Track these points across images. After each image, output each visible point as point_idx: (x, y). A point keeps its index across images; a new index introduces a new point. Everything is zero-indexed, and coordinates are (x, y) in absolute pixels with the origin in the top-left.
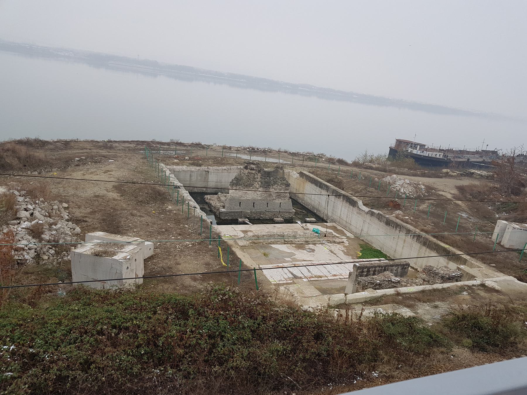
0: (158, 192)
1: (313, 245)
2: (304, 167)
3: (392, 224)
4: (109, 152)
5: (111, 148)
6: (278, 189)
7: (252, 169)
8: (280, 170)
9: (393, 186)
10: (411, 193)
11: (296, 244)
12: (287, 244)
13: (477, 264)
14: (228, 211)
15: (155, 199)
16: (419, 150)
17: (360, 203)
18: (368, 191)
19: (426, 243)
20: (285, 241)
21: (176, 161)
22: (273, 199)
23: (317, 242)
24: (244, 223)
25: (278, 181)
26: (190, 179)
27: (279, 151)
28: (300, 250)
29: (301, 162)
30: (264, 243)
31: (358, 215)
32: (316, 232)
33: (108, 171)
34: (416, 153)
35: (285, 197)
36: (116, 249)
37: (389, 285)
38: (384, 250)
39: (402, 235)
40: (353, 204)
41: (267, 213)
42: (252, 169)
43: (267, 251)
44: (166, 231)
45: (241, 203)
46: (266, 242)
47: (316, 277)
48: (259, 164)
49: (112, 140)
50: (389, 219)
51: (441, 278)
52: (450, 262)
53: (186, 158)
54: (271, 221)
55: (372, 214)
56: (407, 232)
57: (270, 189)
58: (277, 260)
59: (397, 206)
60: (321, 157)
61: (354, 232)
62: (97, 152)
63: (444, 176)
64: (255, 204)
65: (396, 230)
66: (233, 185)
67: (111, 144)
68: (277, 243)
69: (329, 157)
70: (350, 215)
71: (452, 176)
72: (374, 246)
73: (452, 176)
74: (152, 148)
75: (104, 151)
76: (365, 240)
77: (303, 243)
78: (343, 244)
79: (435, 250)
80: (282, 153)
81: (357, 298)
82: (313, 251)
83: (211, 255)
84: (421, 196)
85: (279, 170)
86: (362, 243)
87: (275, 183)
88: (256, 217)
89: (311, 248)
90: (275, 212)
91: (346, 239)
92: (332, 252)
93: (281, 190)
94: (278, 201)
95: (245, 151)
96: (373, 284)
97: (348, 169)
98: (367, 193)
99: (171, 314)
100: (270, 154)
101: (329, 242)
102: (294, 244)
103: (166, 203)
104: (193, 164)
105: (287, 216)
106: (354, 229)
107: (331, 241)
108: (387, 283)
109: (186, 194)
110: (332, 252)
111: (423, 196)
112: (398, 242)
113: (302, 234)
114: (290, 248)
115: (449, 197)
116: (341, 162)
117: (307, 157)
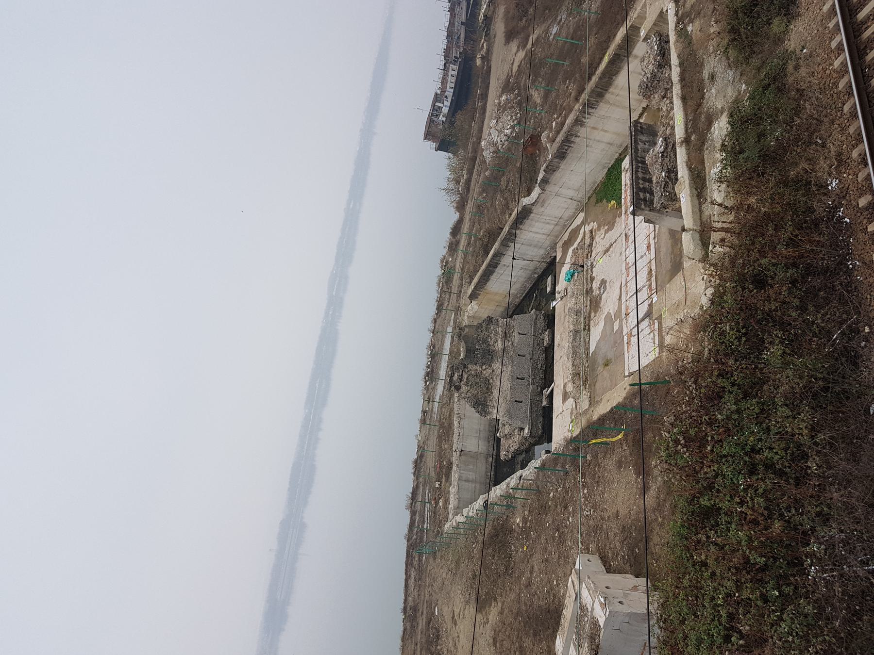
0: (492, 537)
1: (594, 282)
2: (461, 291)
3: (563, 149)
4: (422, 613)
5: (415, 609)
6: (496, 337)
7: (461, 378)
9: (500, 146)
10: (514, 118)
11: (590, 312)
12: (589, 326)
13: (639, 8)
14: (529, 423)
15: (504, 545)
16: (443, 103)
17: (525, 201)
18: (506, 187)
19: (600, 93)
20: (584, 329)
21: (441, 504)
22: (513, 345)
23: (589, 275)
24: (551, 396)
26: (472, 481)
27: (433, 333)
28: (601, 305)
29: (454, 296)
30: (587, 365)
31: (546, 205)
32: (572, 276)
33: (453, 617)
34: (447, 109)
36: (586, 619)
37: (670, 157)
38: (608, 162)
39: (582, 132)
40: (525, 213)
41: (535, 357)
43: (600, 361)
44: (558, 530)
45: (517, 399)
46: (585, 361)
47: (650, 280)
48: (453, 367)
49: (402, 606)
50: (555, 154)
51: (661, 68)
52: (633, 53)
53: (437, 486)
54: (549, 351)
55: (545, 181)
56: (578, 124)
57: (494, 351)
58: (617, 345)
59: (534, 141)
60: (447, 263)
61: (574, 213)
62: (422, 633)
63: (488, 63)
64: (518, 377)
65: (575, 143)
66: (485, 412)
67: (408, 609)
68: (587, 342)
69: (446, 250)
70: (545, 218)
71: (488, 50)
72: (600, 179)
73: (489, 51)
74: (418, 541)
75: (420, 622)
76: (589, 195)
77: (589, 298)
78: (594, 232)
79: (612, 79)
80: (437, 327)
81: (691, 211)
82: (603, 282)
83: (604, 457)
84: (519, 100)
85: (464, 333)
86: (593, 200)
87: (485, 341)
89: (598, 285)
90: (533, 344)
91: (586, 226)
92: (607, 251)
93: (497, 333)
94: (516, 337)
95: (430, 387)
96: (666, 183)
97: (468, 219)
98: (509, 190)
99: (708, 537)
100: (437, 347)
101: (589, 255)
102: (590, 314)
103: (511, 527)
104: (448, 475)
105: (541, 323)
106: (570, 212)
107: (589, 252)
108: (667, 160)
109: (498, 491)
110: (607, 251)
111: (519, 98)
112: (595, 140)
113: (573, 299)
114: (597, 321)
115: (524, 55)
116: (456, 230)
117: (445, 287)
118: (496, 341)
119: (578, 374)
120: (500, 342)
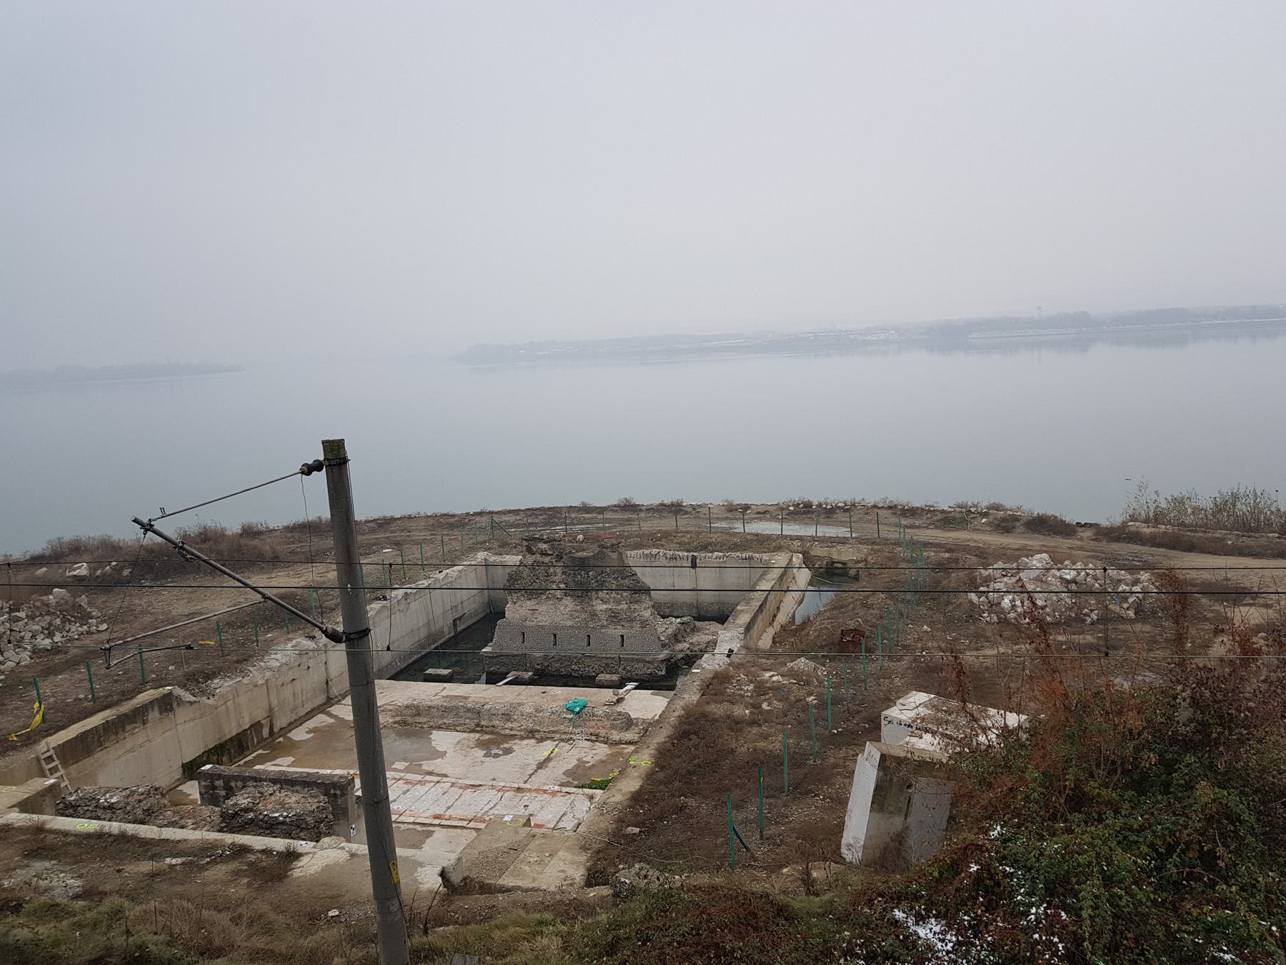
6: (612, 600)
7: (544, 554)
8: (611, 554)
22: (603, 626)
25: (609, 579)
30: (425, 726)
35: (632, 621)
42: (544, 554)
46: (431, 724)
88: (563, 670)
90: (607, 658)
93: (619, 603)
94: (615, 631)
118: (604, 601)
119: (419, 715)
120: (605, 607)
